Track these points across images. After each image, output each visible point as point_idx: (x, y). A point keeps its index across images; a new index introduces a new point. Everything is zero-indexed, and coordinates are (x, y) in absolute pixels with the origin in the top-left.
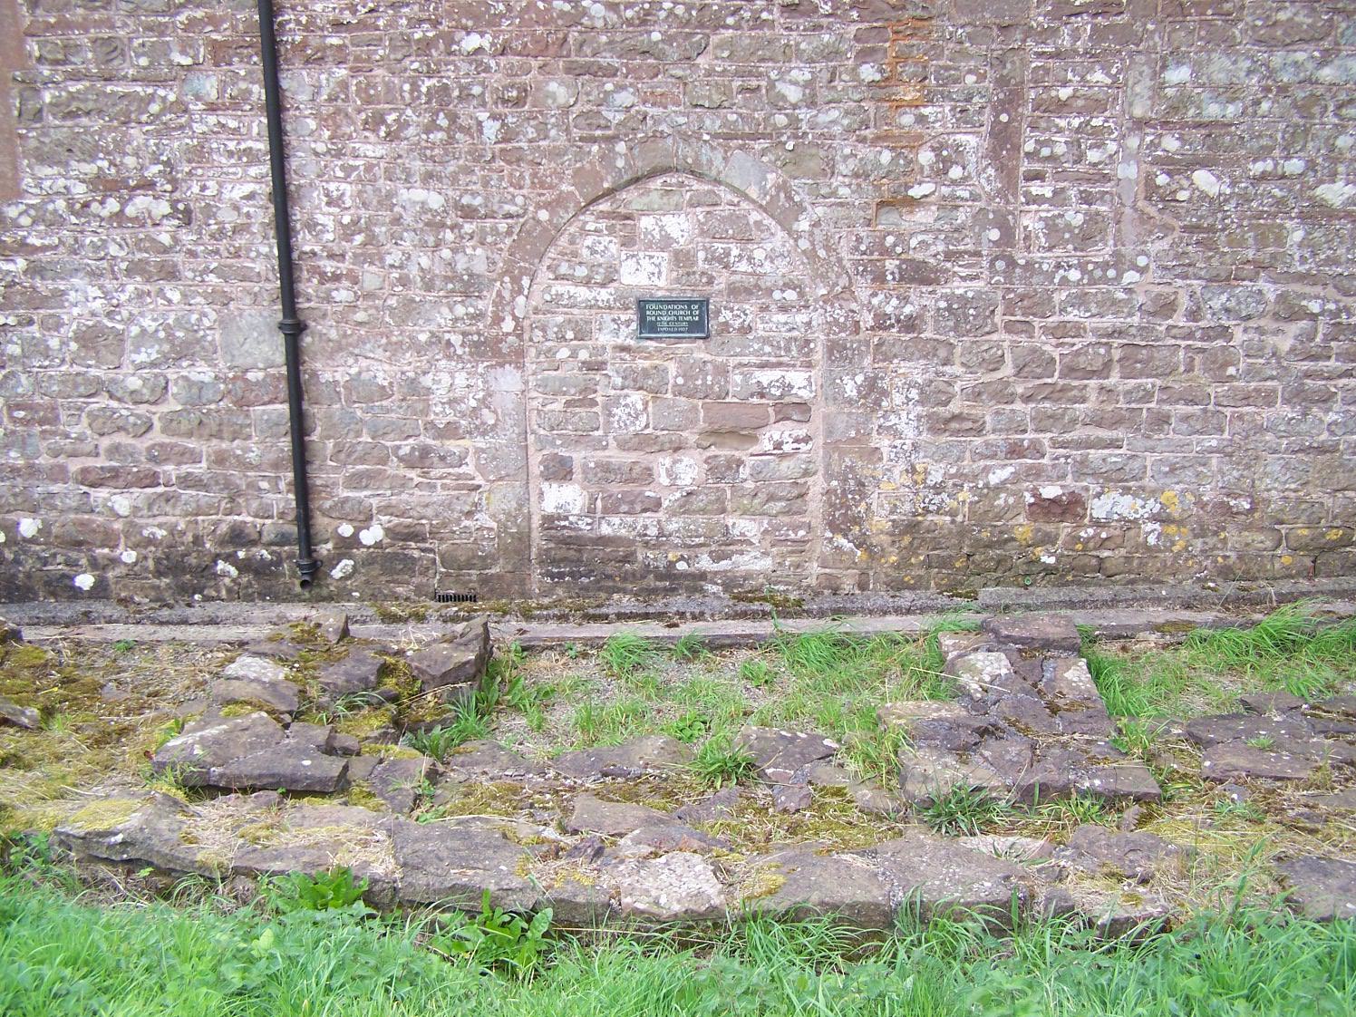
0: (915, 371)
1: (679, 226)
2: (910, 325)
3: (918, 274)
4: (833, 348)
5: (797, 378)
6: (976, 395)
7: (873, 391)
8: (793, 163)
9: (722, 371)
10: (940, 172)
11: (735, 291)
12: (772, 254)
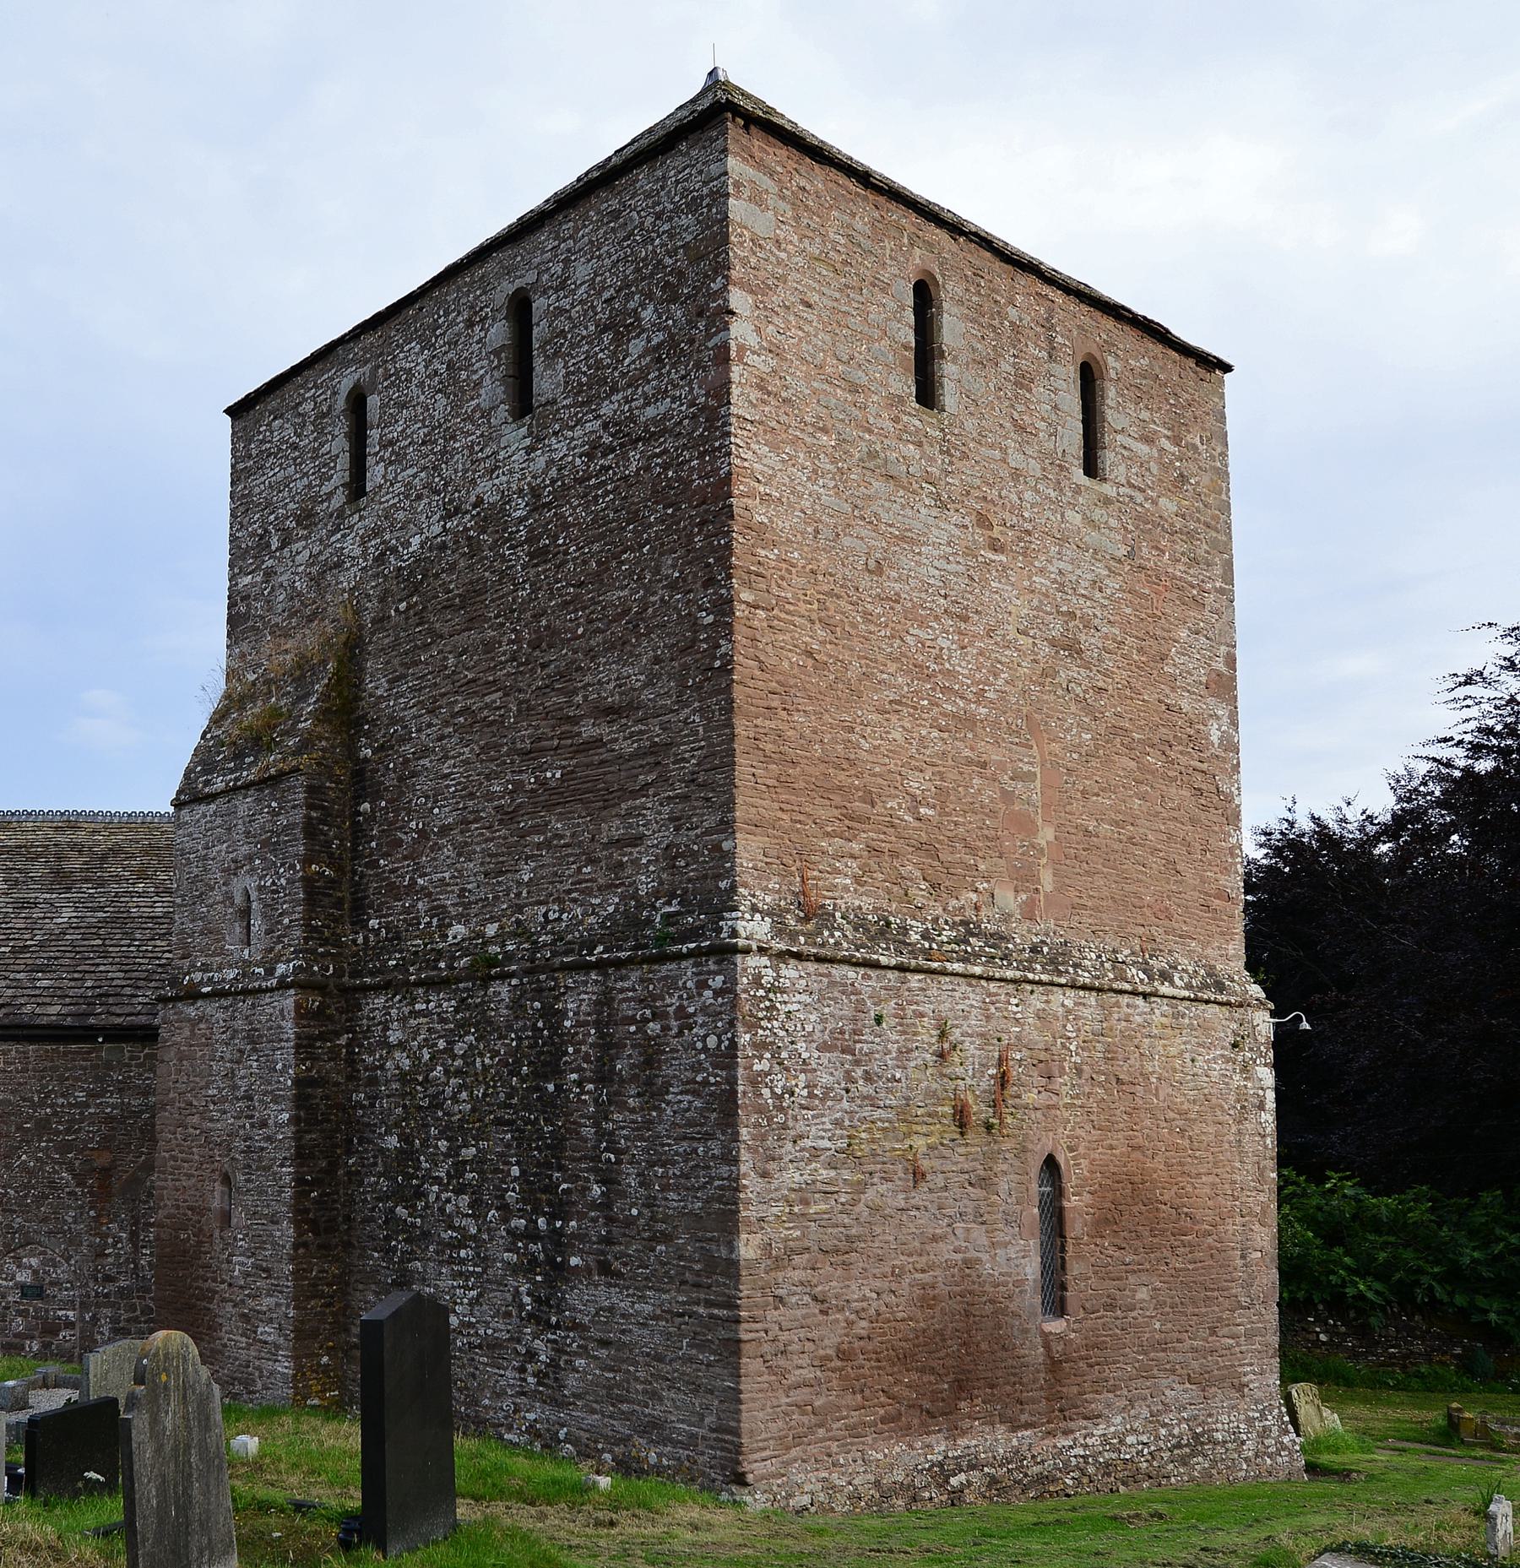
0: (107, 1312)
1: (34, 1262)
2: (107, 1296)
3: (108, 1279)
4: (81, 1303)
5: (71, 1313)
6: (128, 1320)
7: (95, 1319)
8: (71, 1242)
9: (47, 1311)
10: (114, 1246)
11: (52, 1284)
12: (62, 1273)
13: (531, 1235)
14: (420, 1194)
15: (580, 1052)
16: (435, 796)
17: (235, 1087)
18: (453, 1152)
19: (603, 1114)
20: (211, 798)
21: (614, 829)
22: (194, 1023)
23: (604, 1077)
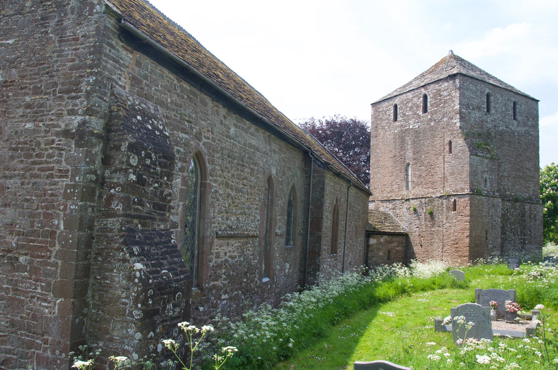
13: (521, 239)
14: (505, 233)
15: (527, 214)
16: (505, 171)
17: (489, 214)
18: (510, 227)
19: (530, 223)
20: (479, 156)
21: (528, 185)
22: (479, 200)
23: (530, 218)
